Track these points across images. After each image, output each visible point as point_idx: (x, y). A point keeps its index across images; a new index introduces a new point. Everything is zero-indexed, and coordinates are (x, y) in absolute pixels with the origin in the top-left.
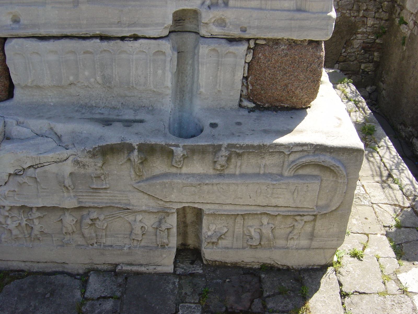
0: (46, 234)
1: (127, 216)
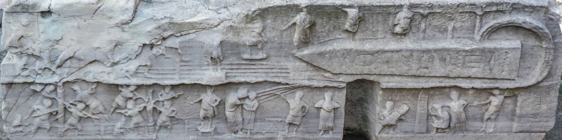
0: (177, 120)
1: (284, 94)
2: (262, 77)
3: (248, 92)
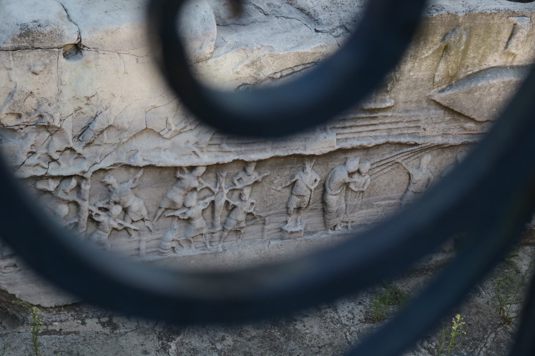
1: (406, 161)
2: (383, 137)
3: (359, 163)
